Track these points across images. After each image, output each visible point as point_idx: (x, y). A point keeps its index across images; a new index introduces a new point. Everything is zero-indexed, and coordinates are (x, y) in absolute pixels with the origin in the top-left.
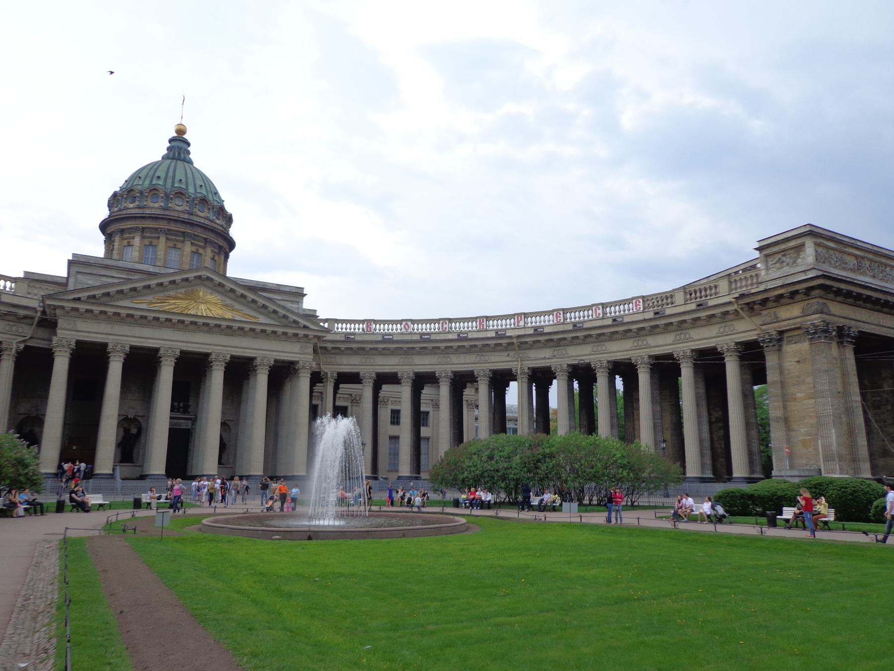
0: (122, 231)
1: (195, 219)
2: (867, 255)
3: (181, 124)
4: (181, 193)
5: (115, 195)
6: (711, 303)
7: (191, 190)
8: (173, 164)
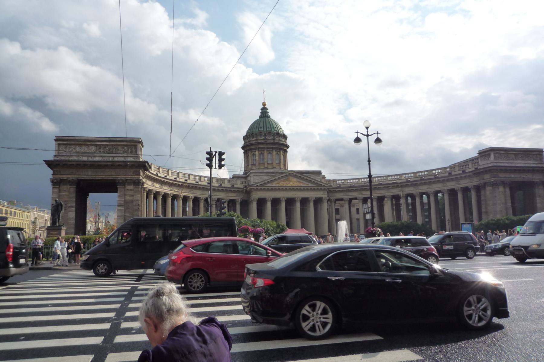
0: (251, 149)
1: (276, 141)
2: (519, 153)
3: (264, 102)
4: (270, 132)
5: (246, 135)
6: (467, 171)
7: (273, 130)
8: (265, 120)
